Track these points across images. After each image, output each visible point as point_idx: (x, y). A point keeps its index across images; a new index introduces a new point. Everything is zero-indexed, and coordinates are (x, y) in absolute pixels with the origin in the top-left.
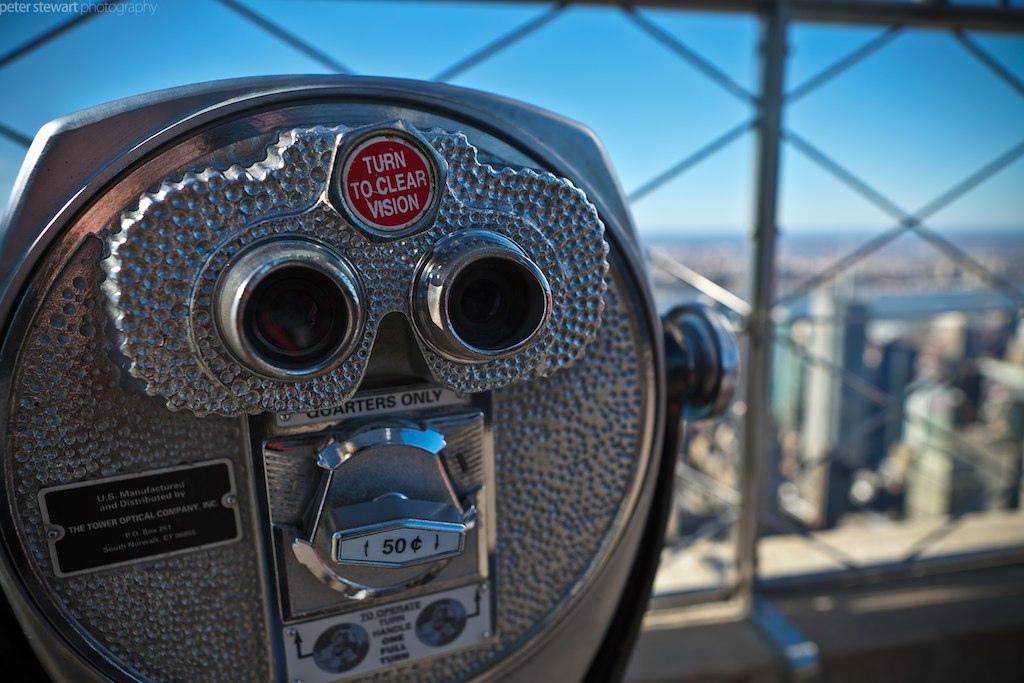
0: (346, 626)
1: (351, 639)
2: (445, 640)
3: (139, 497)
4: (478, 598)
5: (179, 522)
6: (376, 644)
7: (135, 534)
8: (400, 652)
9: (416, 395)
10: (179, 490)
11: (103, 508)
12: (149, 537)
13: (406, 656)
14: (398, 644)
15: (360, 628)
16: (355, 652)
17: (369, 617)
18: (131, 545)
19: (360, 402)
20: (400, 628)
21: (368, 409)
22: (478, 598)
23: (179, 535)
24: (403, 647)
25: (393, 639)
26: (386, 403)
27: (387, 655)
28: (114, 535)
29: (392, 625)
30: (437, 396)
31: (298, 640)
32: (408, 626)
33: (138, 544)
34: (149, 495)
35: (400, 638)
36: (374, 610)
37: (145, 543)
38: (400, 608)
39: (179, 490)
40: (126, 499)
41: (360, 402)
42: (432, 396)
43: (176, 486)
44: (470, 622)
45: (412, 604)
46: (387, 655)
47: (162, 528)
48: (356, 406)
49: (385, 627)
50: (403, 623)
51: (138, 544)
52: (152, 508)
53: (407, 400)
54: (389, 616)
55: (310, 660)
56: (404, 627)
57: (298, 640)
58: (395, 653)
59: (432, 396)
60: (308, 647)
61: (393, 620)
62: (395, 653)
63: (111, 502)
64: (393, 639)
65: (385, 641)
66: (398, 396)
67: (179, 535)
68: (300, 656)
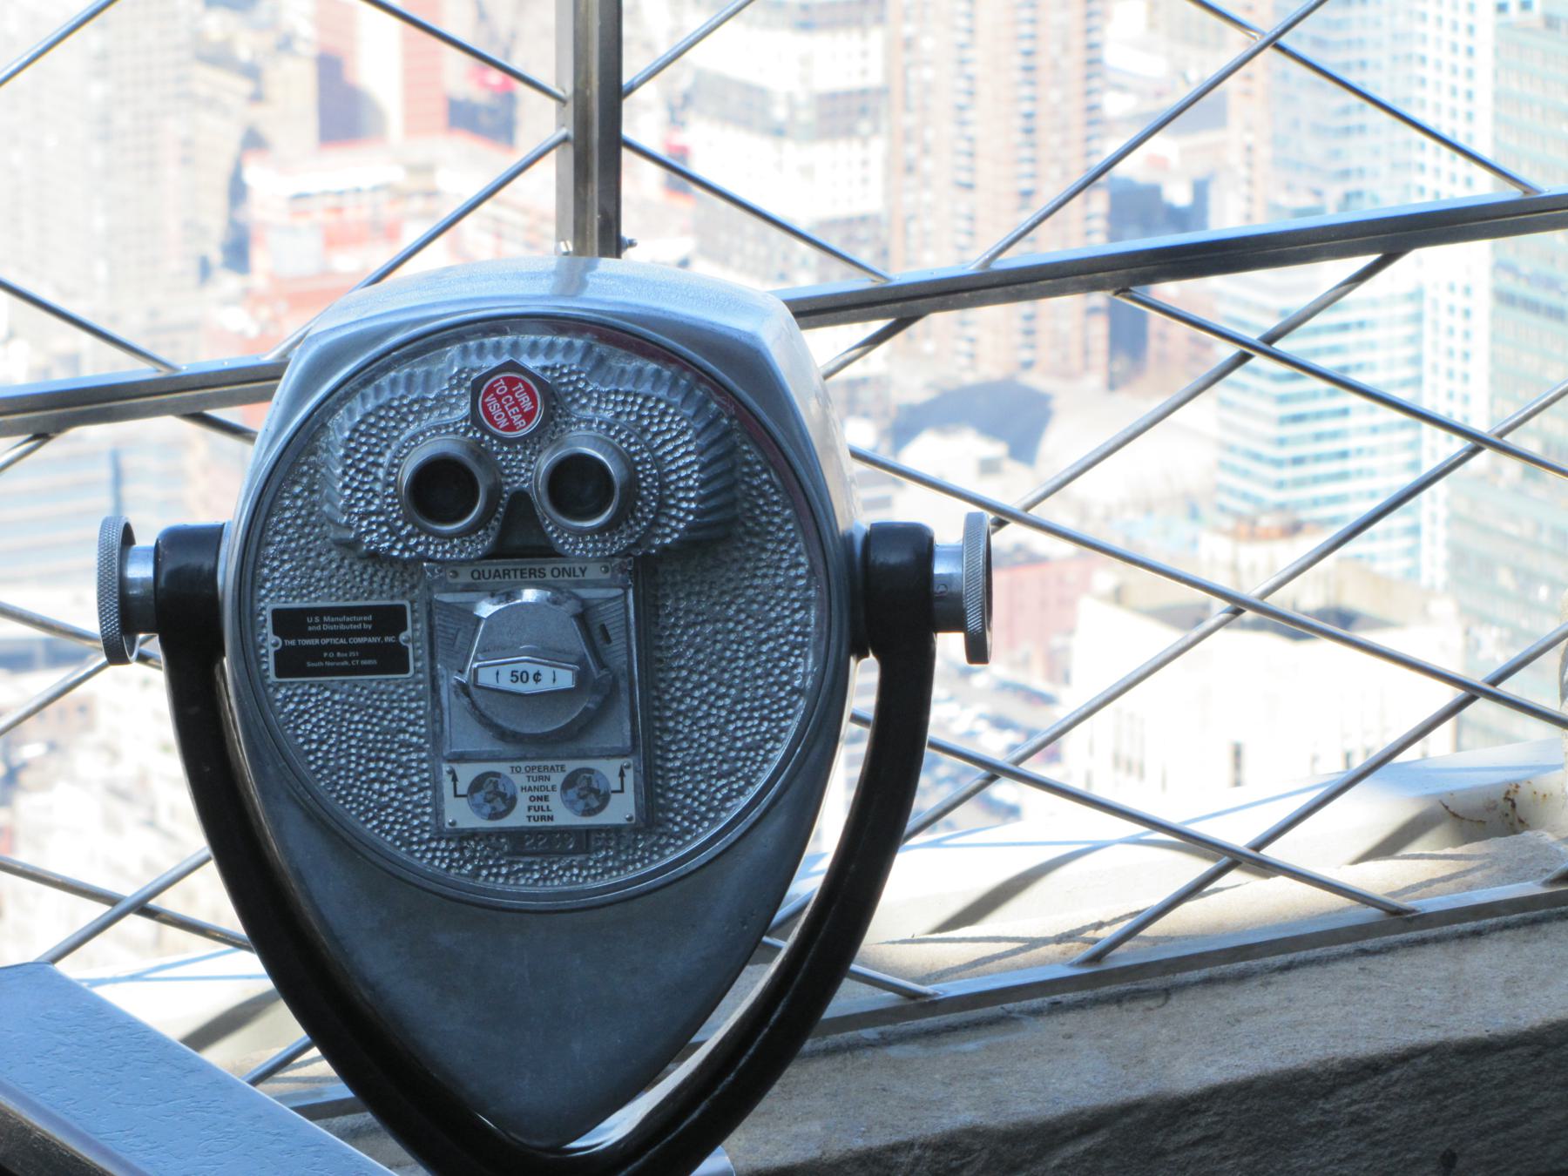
0: (497, 775)
1: (501, 789)
2: (589, 812)
3: (337, 623)
4: (622, 775)
5: (366, 651)
6: (523, 800)
7: (331, 655)
8: (546, 814)
9: (564, 569)
10: (368, 622)
11: (310, 628)
12: (341, 659)
13: (551, 818)
14: (544, 804)
15: (509, 780)
16: (504, 803)
17: (517, 770)
18: (328, 664)
19: (515, 570)
20: (546, 788)
21: (522, 577)
22: (622, 775)
23: (364, 662)
24: (548, 810)
25: (539, 798)
26: (537, 574)
27: (532, 813)
28: (316, 653)
29: (538, 784)
30: (583, 572)
31: (455, 779)
32: (553, 788)
33: (332, 664)
34: (346, 623)
35: (546, 798)
36: (523, 764)
37: (338, 664)
38: (546, 768)
39: (368, 622)
40: (327, 623)
41: (515, 570)
42: (578, 572)
43: (365, 618)
44: (614, 797)
45: (557, 766)
46: (532, 813)
47: (352, 654)
48: (512, 574)
49: (532, 784)
50: (549, 784)
51: (332, 664)
52: (347, 634)
53: (556, 573)
54: (535, 774)
55: (464, 799)
56: (550, 788)
57: (455, 779)
58: (540, 813)
59: (578, 572)
60: (463, 788)
61: (540, 778)
62: (540, 813)
63: (316, 624)
64: (539, 798)
65: (532, 799)
66: (548, 568)
67: (364, 662)
68: (456, 795)
